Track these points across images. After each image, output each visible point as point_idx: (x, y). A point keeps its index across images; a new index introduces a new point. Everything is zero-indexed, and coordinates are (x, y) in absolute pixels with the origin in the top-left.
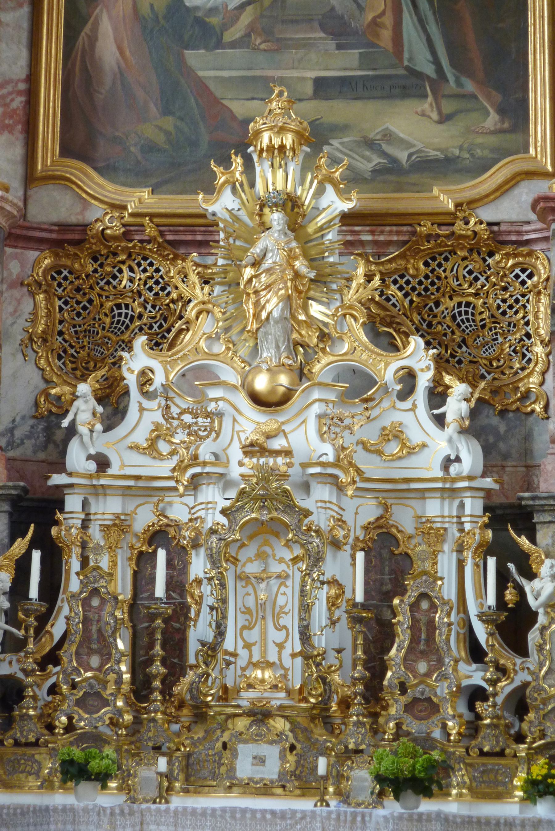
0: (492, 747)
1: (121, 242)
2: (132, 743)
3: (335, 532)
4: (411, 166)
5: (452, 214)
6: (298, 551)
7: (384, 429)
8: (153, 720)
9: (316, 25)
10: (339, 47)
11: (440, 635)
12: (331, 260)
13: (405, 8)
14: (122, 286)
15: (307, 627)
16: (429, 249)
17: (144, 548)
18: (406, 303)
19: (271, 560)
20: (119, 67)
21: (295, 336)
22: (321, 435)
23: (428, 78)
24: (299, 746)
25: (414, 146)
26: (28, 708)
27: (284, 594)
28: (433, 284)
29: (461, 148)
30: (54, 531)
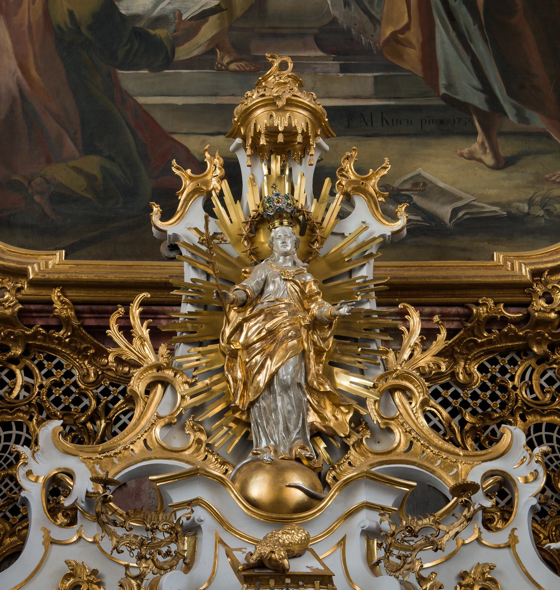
1: (14, 326)
4: (457, 225)
5: (528, 285)
7: (463, 575)
9: (310, 40)
10: (344, 69)
12: (367, 306)
13: (437, 21)
14: (15, 393)
16: (490, 342)
18: (455, 424)
20: (21, 90)
21: (312, 418)
22: (373, 566)
23: (477, 110)
25: (460, 199)
28: (494, 397)
29: (530, 202)
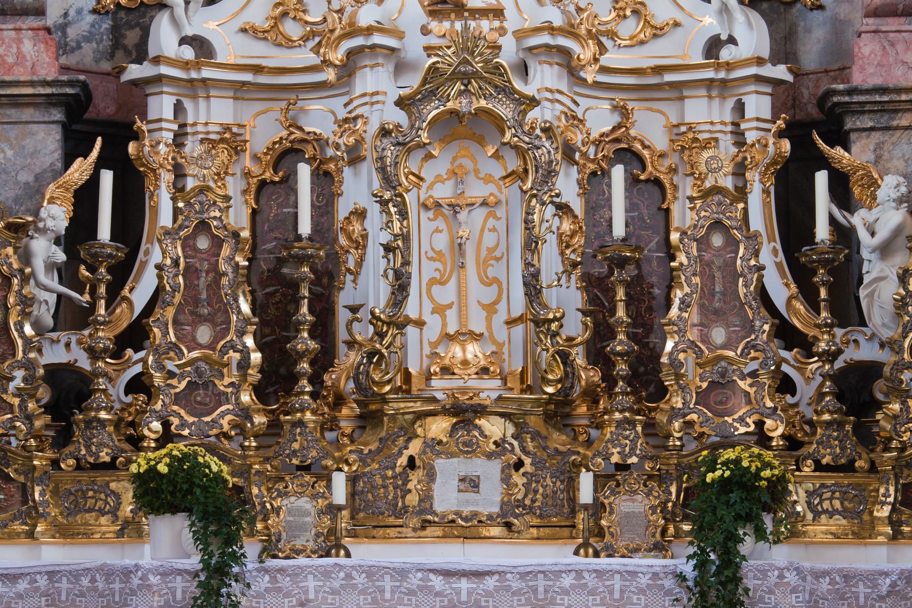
0: (835, 457)
2: (267, 460)
3: (570, 135)
6: (513, 163)
8: (301, 423)
11: (746, 286)
15: (536, 275)
17: (267, 175)
19: (471, 178)
24: (528, 461)
26: (99, 409)
27: (494, 230)
30: (132, 148)
